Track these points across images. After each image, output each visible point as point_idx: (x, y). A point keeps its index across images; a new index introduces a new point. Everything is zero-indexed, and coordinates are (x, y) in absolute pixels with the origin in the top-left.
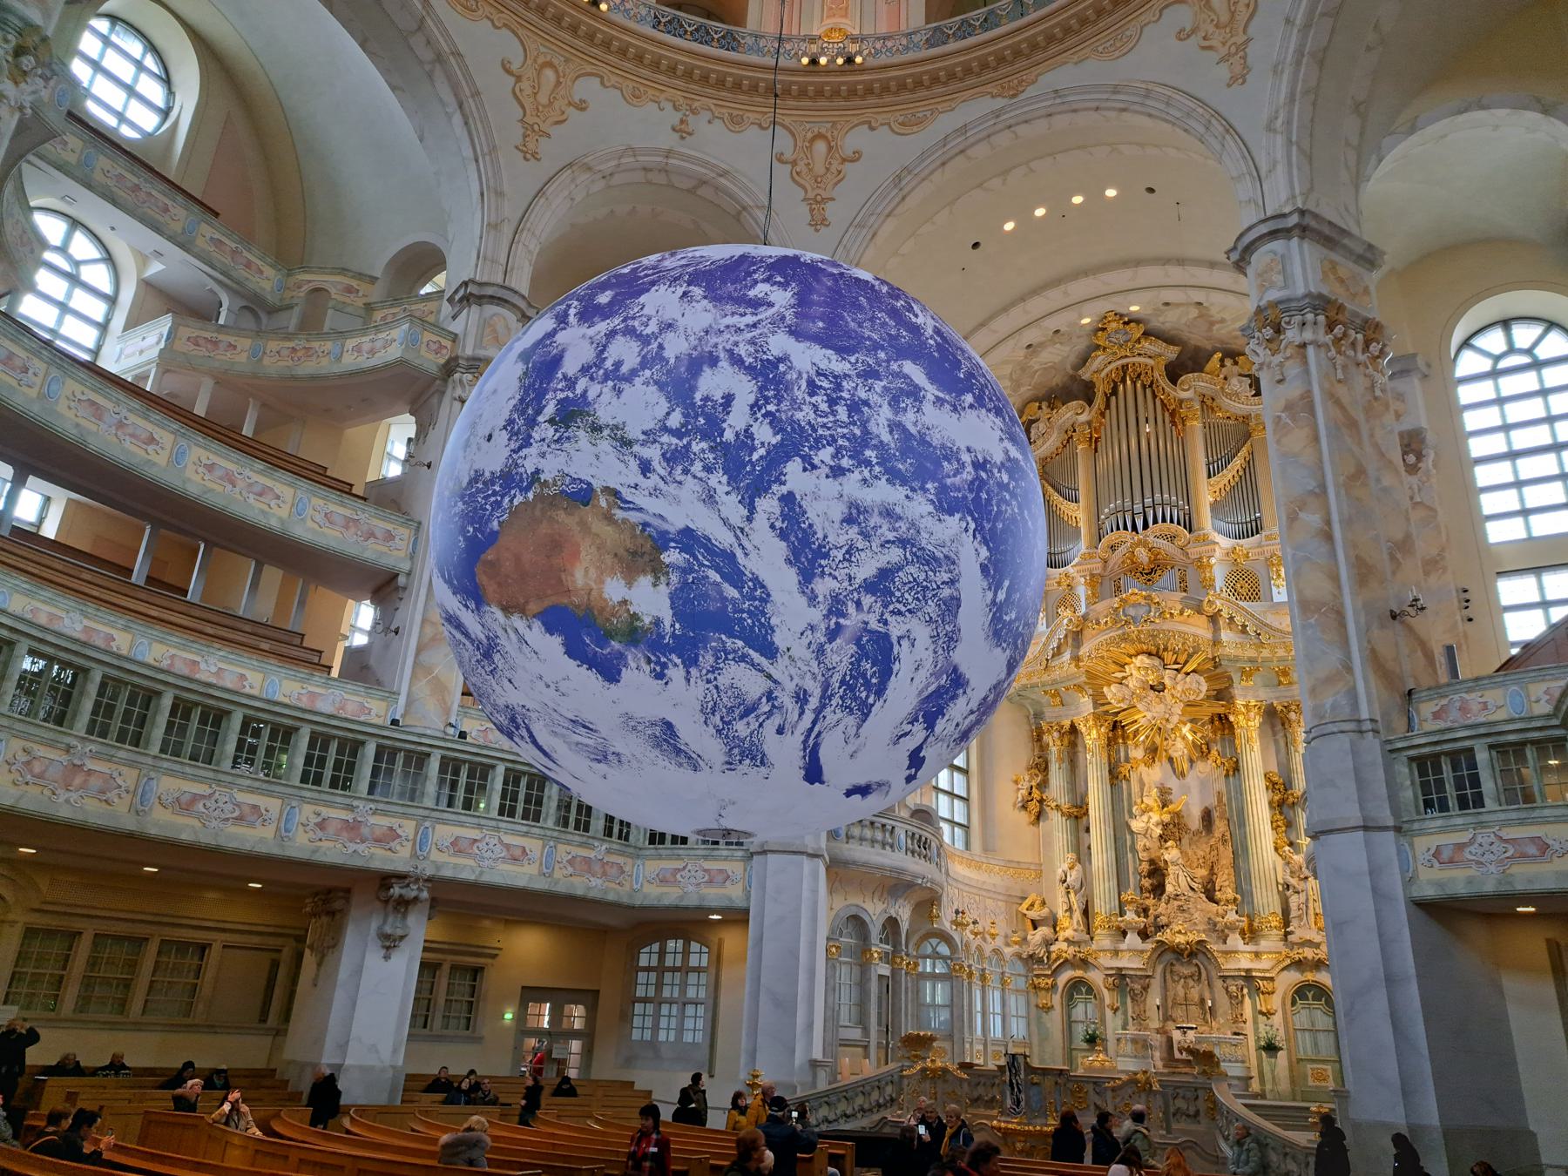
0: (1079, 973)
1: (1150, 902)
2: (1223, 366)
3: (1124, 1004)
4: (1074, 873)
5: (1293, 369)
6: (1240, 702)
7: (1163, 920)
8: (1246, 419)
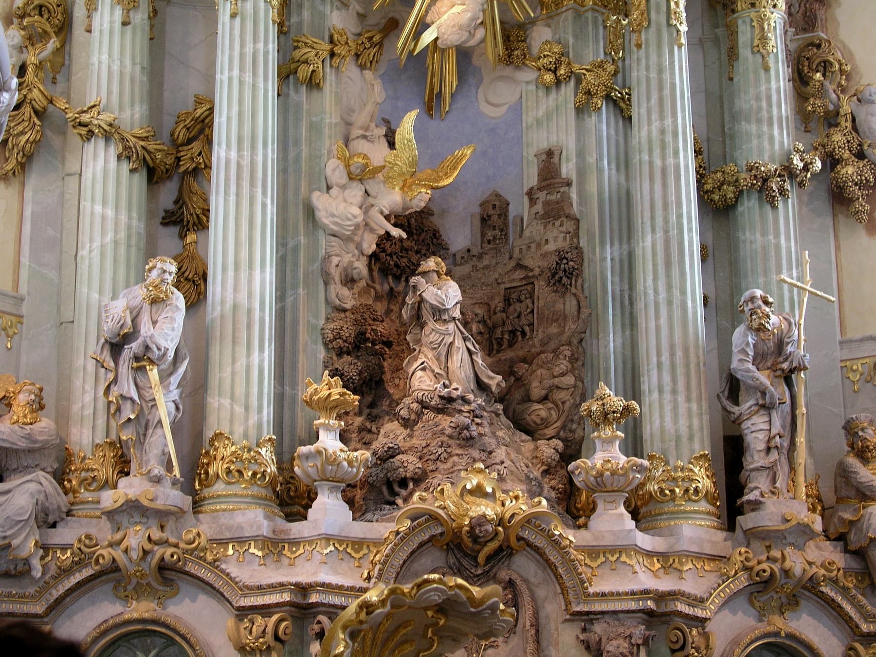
4: (166, 313)
7: (410, 463)
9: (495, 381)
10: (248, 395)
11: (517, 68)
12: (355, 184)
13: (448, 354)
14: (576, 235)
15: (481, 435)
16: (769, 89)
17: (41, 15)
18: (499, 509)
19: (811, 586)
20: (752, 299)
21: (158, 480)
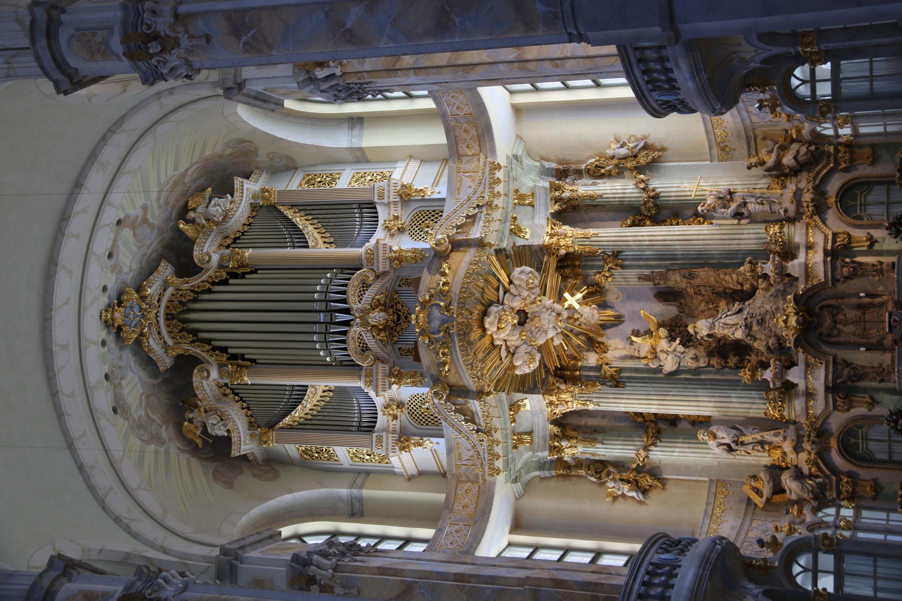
0: (833, 443)
1: (753, 359)
2: (193, 221)
3: (866, 390)
4: (720, 434)
5: (200, 26)
6: (547, 240)
7: (772, 341)
8: (254, 207)
17: (600, 472)
18: (792, 314)
21: (785, 438)
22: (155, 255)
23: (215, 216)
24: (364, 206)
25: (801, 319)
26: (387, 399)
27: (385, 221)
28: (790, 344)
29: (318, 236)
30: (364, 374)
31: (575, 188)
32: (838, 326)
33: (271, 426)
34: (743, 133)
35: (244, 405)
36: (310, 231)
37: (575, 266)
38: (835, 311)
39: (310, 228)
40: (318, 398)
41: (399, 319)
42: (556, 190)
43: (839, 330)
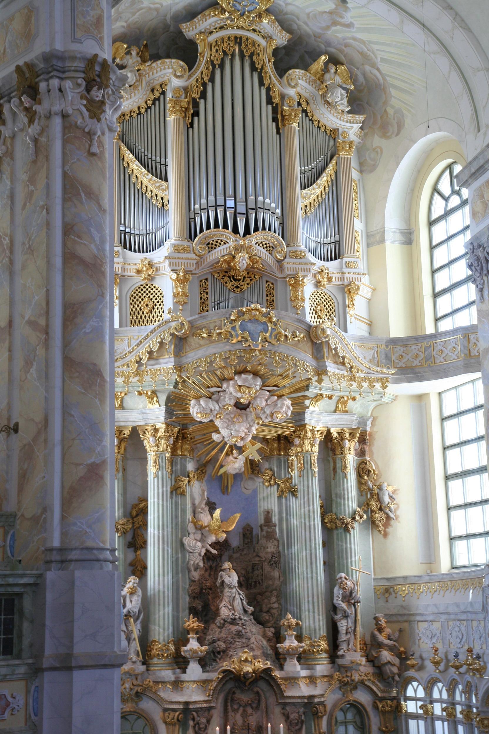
2: (326, 69)
9: (251, 609)
10: (164, 624)
11: (257, 475)
12: (199, 532)
13: (233, 600)
14: (278, 547)
15: (246, 633)
16: (347, 486)
19: (362, 682)
20: (341, 578)
22: (295, 27)
23: (332, 94)
24: (337, 246)
25: (250, 675)
26: (158, 265)
27: (328, 269)
28: (225, 665)
29: (311, 200)
30: (186, 243)
31: (352, 452)
32: (241, 709)
33: (121, 137)
34: (406, 612)
35: (143, 111)
36: (315, 191)
37: (279, 450)
38: (254, 705)
39: (318, 192)
40: (155, 191)
41: (235, 280)
42: (350, 434)
43: (237, 710)
